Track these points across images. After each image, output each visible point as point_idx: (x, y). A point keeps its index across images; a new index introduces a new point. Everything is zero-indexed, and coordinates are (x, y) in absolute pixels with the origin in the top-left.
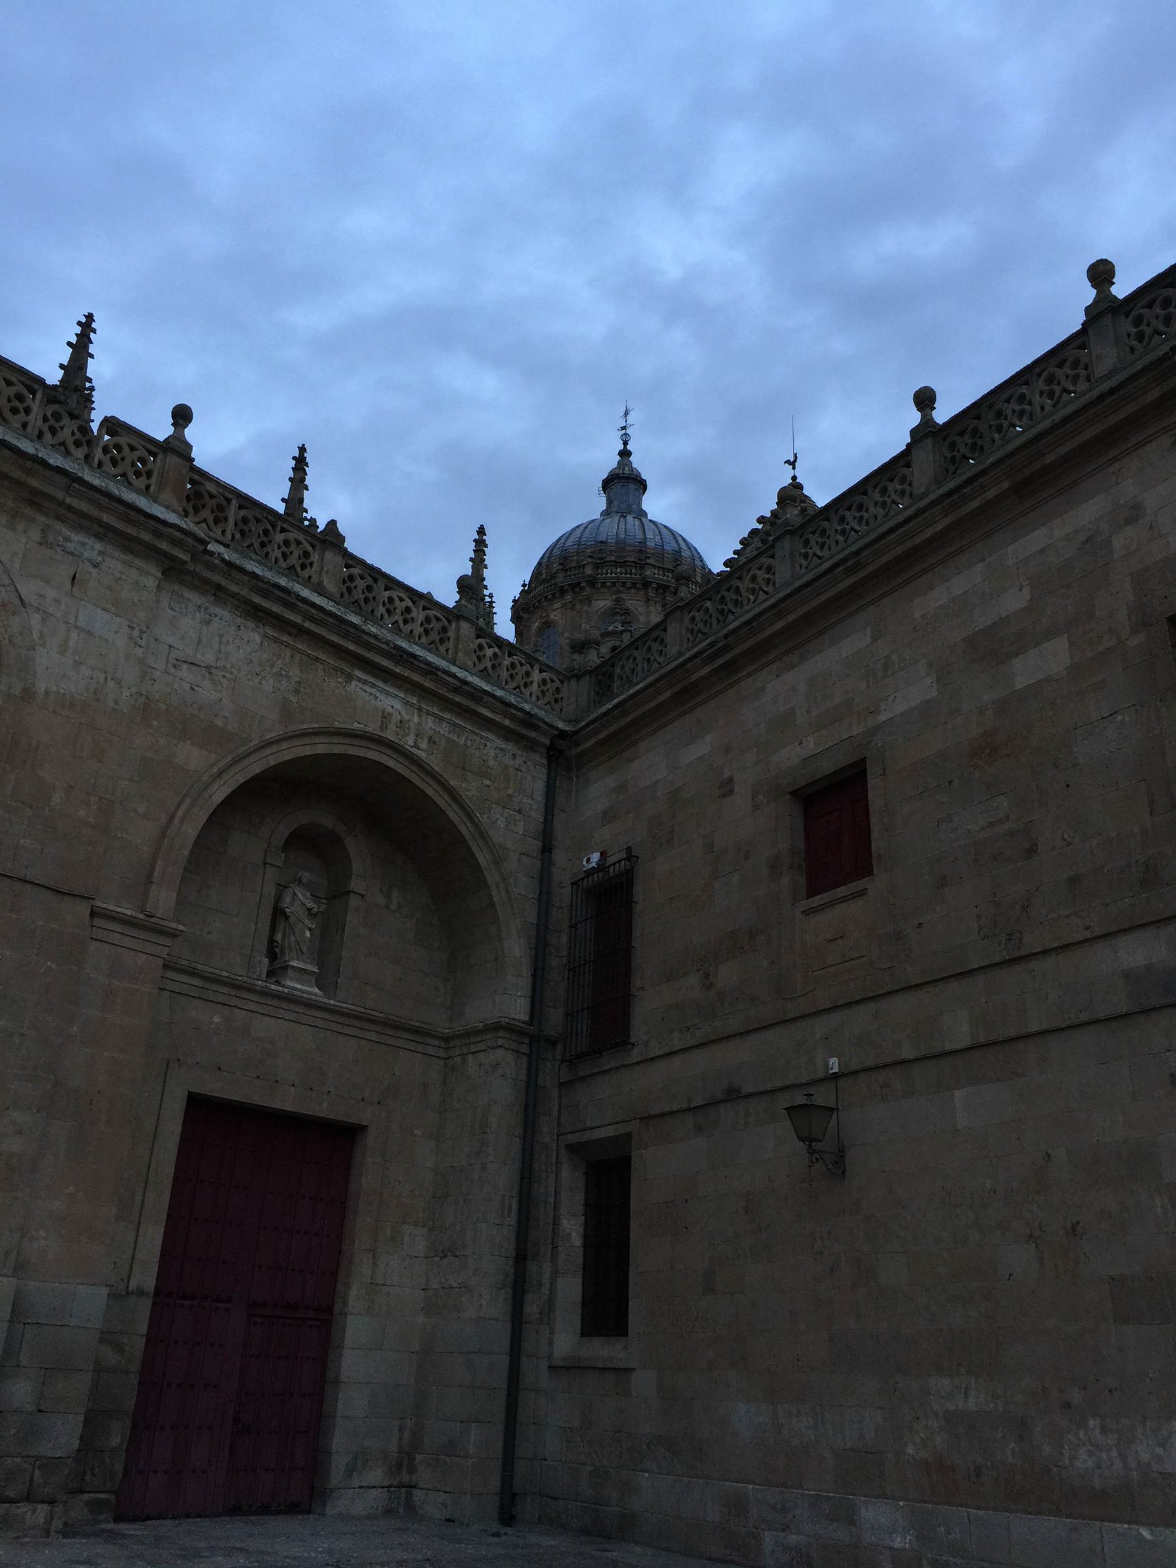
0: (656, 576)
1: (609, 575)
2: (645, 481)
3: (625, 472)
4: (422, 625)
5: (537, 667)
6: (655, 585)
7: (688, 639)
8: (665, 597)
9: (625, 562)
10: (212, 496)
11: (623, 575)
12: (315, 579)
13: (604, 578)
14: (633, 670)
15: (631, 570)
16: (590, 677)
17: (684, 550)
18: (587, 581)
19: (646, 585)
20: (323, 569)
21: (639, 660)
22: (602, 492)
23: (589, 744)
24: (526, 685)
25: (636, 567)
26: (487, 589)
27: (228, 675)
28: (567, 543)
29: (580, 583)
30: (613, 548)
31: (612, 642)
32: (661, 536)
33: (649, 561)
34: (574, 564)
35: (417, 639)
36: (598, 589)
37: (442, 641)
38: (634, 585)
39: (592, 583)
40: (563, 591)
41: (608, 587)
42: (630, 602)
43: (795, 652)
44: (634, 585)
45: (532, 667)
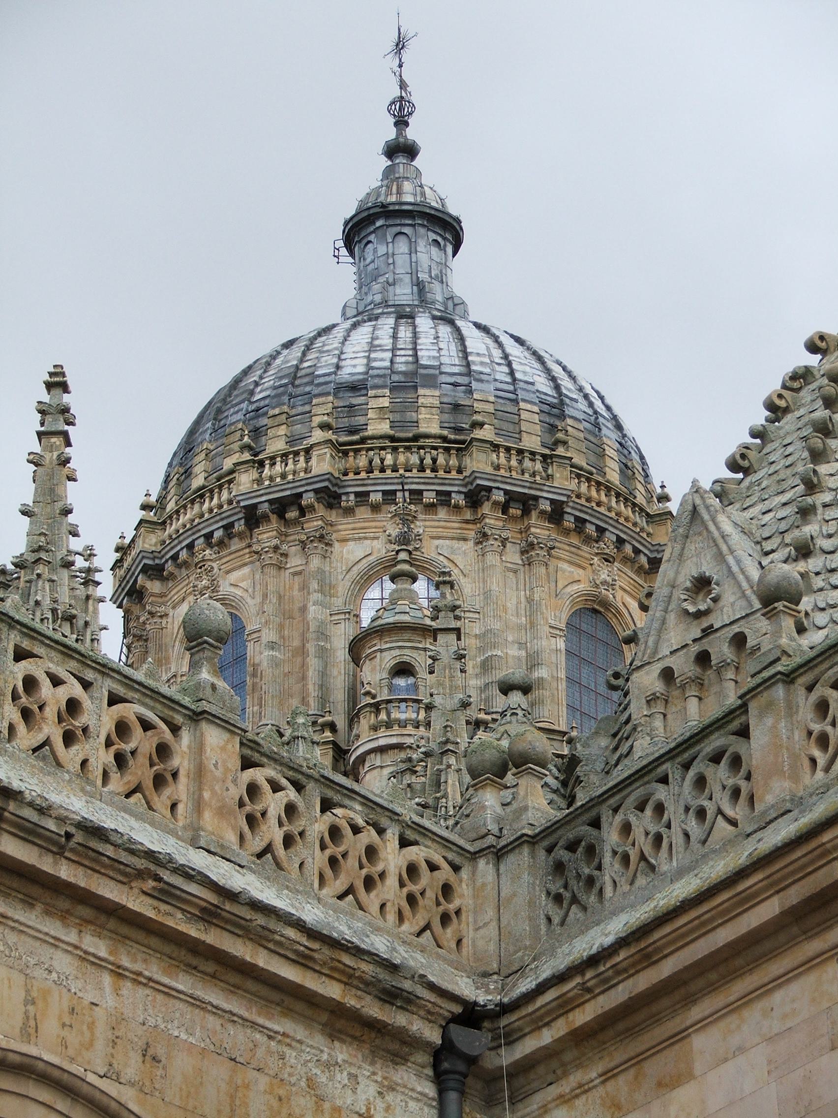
2: (459, 222)
4: (109, 743)
5: (392, 834)
6: (499, 497)
7: (813, 761)
8: (528, 528)
9: (416, 438)
14: (658, 840)
15: (434, 460)
16: (533, 854)
17: (572, 399)
18: (316, 491)
21: (673, 811)
22: (344, 251)
23: (547, 1037)
24: (369, 884)
25: (447, 450)
26: (75, 534)
29: (299, 496)
31: (397, 652)
33: (479, 434)
35: (99, 782)
37: (159, 781)
38: (444, 498)
44: (444, 498)
45: (381, 831)
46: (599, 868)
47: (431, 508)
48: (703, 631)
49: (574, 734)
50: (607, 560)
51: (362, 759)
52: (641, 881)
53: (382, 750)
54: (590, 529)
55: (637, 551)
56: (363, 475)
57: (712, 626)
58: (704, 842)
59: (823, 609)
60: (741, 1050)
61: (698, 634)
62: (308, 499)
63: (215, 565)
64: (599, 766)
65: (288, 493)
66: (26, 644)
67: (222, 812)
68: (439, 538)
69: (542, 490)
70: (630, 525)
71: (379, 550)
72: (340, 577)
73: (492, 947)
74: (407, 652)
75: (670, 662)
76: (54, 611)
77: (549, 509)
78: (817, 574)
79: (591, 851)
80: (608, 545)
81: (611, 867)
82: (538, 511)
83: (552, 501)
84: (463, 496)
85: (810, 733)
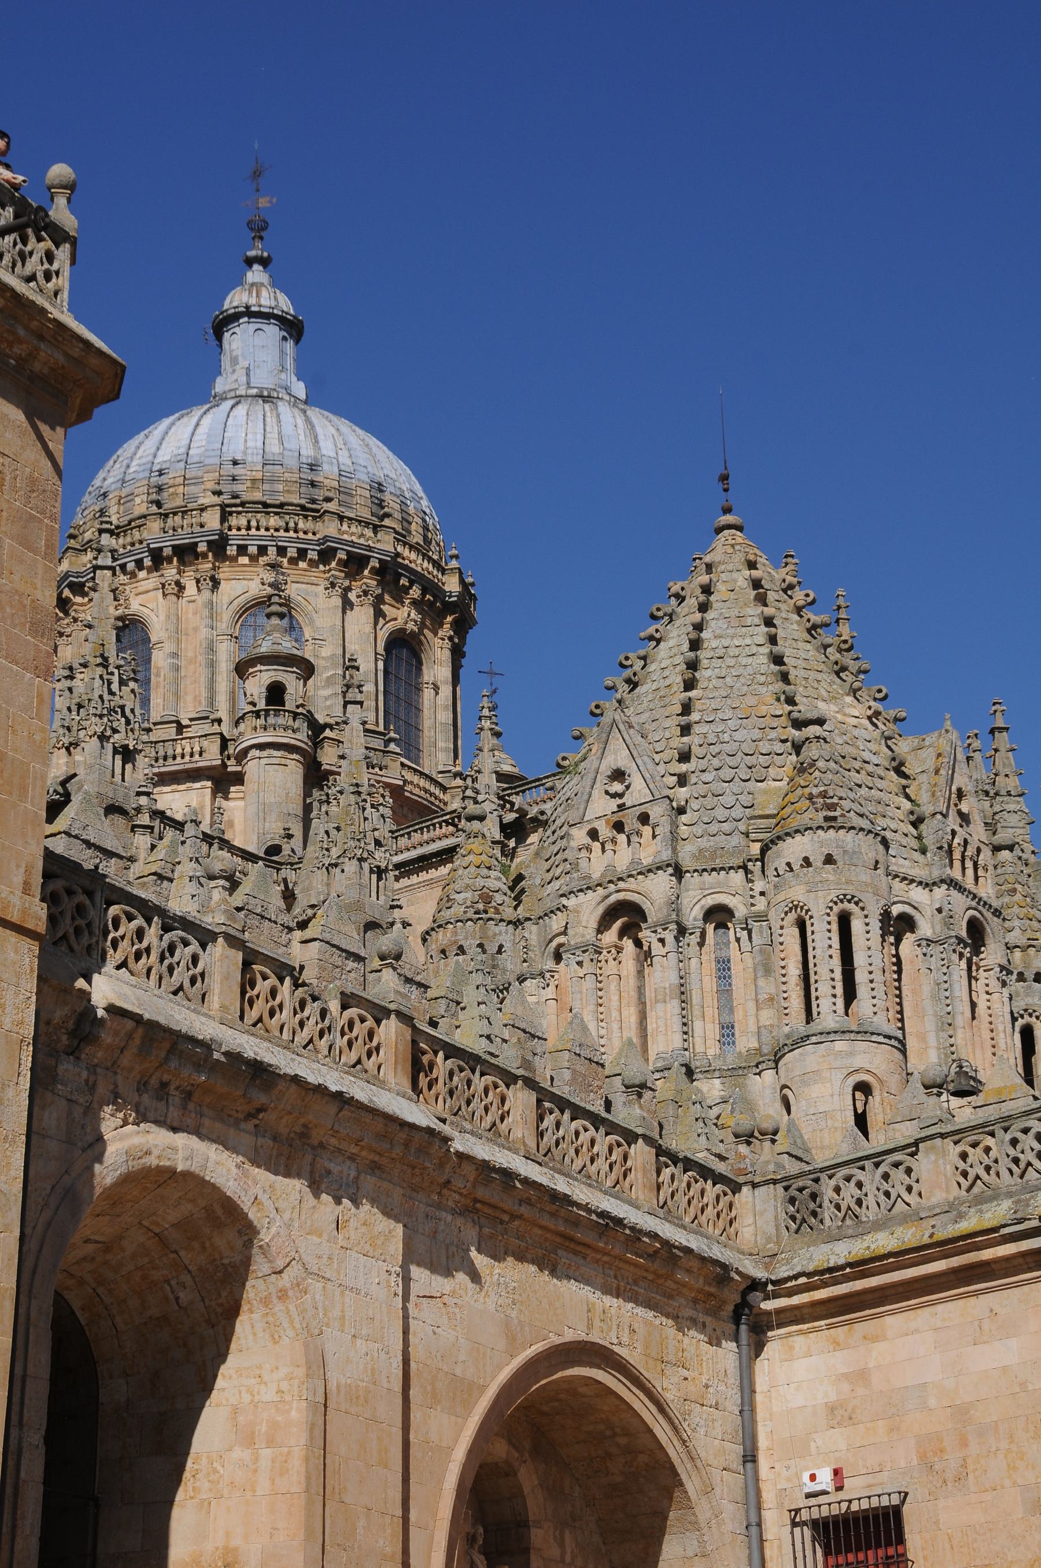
3: (263, 302)
9: (281, 505)
11: (282, 533)
14: (859, 1203)
15: (296, 524)
25: (306, 517)
27: (458, 1301)
28: (160, 453)
29: (196, 544)
30: (259, 475)
31: (273, 673)
32: (349, 450)
33: (327, 506)
34: (179, 502)
40: (158, 559)
44: (302, 553)
46: (820, 1206)
47: (293, 561)
48: (619, 806)
49: (392, 734)
51: (245, 751)
52: (848, 1222)
53: (261, 747)
56: (243, 532)
57: (624, 804)
58: (889, 1211)
60: (917, 1331)
61: (616, 809)
62: (202, 547)
64: (538, 881)
65: (187, 541)
72: (225, 607)
74: (280, 673)
75: (596, 824)
77: (377, 565)
79: (814, 1196)
80: (415, 592)
81: (828, 1212)
83: (380, 560)
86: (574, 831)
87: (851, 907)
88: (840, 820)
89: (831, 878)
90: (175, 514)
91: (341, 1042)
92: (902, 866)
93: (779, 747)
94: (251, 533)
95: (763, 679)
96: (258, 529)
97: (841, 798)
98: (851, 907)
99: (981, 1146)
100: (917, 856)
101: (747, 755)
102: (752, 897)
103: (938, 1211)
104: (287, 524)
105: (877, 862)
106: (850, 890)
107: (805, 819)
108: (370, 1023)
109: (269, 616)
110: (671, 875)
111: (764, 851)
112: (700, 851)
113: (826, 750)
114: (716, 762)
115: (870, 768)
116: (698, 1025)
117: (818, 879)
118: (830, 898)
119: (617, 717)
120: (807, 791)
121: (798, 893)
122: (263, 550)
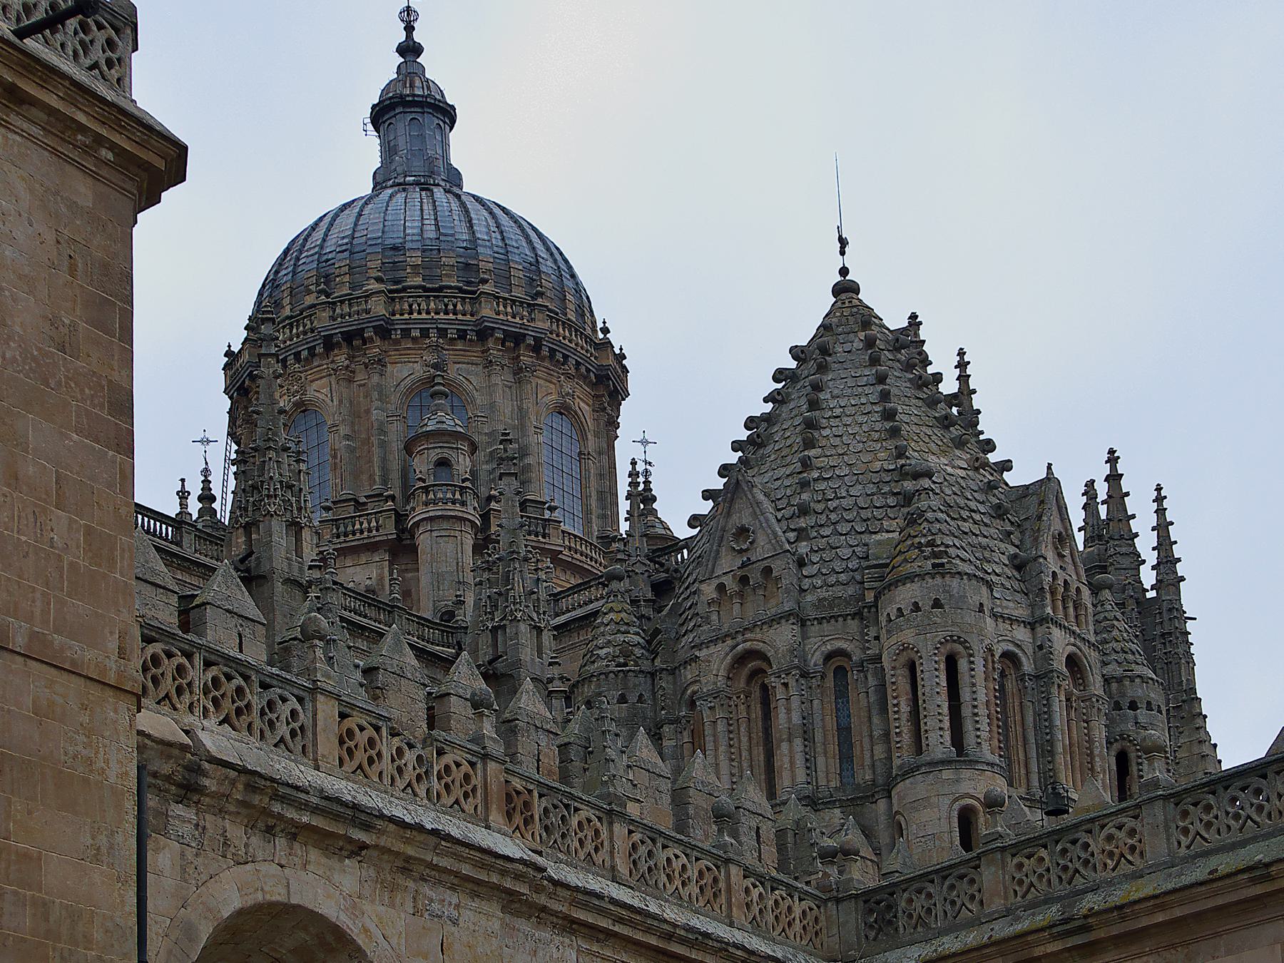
0: (501, 317)
1: (415, 315)
7: (1015, 892)
8: (518, 356)
9: (441, 289)
10: (518, 793)
11: (442, 316)
12: (608, 864)
13: (406, 322)
14: (929, 911)
15: (455, 306)
16: (856, 903)
19: (484, 334)
20: (614, 848)
21: (937, 898)
36: (397, 342)
38: (462, 335)
39: (384, 331)
40: (329, 344)
41: (414, 339)
42: (458, 366)
43: (1179, 949)
44: (462, 335)
50: (569, 378)
52: (919, 929)
54: (559, 357)
55: (588, 370)
58: (955, 918)
59: (816, 551)
63: (302, 375)
65: (354, 327)
66: (665, 842)
67: (739, 907)
68: (459, 363)
69: (528, 330)
70: (584, 352)
71: (418, 371)
73: (837, 946)
75: (724, 580)
76: (281, 482)
78: (812, 527)
82: (525, 345)
84: (475, 333)
85: (1014, 878)
86: (704, 587)
87: (959, 648)
88: (947, 566)
89: (939, 620)
90: (342, 302)
91: (436, 785)
92: (1007, 608)
93: (891, 501)
94: (413, 317)
95: (876, 436)
96: (419, 313)
97: (947, 546)
98: (959, 648)
99: (1036, 856)
100: (1018, 597)
101: (863, 508)
102: (868, 641)
103: (996, 916)
104: (446, 305)
105: (981, 605)
106: (956, 631)
107: (913, 568)
108: (466, 767)
109: (433, 396)
110: (793, 624)
111: (877, 598)
112: (820, 600)
113: (935, 502)
114: (833, 517)
115: (977, 517)
116: (821, 761)
117: (926, 622)
118: (938, 639)
119: (740, 478)
120: (917, 540)
121: (908, 636)
122: (425, 333)
